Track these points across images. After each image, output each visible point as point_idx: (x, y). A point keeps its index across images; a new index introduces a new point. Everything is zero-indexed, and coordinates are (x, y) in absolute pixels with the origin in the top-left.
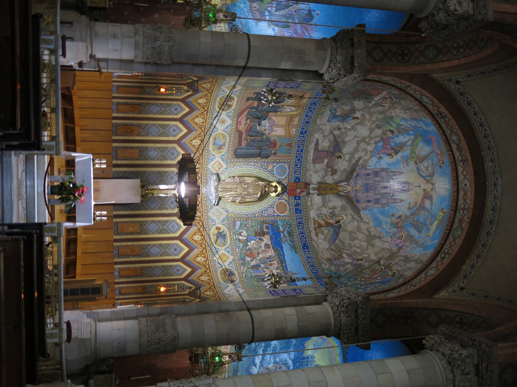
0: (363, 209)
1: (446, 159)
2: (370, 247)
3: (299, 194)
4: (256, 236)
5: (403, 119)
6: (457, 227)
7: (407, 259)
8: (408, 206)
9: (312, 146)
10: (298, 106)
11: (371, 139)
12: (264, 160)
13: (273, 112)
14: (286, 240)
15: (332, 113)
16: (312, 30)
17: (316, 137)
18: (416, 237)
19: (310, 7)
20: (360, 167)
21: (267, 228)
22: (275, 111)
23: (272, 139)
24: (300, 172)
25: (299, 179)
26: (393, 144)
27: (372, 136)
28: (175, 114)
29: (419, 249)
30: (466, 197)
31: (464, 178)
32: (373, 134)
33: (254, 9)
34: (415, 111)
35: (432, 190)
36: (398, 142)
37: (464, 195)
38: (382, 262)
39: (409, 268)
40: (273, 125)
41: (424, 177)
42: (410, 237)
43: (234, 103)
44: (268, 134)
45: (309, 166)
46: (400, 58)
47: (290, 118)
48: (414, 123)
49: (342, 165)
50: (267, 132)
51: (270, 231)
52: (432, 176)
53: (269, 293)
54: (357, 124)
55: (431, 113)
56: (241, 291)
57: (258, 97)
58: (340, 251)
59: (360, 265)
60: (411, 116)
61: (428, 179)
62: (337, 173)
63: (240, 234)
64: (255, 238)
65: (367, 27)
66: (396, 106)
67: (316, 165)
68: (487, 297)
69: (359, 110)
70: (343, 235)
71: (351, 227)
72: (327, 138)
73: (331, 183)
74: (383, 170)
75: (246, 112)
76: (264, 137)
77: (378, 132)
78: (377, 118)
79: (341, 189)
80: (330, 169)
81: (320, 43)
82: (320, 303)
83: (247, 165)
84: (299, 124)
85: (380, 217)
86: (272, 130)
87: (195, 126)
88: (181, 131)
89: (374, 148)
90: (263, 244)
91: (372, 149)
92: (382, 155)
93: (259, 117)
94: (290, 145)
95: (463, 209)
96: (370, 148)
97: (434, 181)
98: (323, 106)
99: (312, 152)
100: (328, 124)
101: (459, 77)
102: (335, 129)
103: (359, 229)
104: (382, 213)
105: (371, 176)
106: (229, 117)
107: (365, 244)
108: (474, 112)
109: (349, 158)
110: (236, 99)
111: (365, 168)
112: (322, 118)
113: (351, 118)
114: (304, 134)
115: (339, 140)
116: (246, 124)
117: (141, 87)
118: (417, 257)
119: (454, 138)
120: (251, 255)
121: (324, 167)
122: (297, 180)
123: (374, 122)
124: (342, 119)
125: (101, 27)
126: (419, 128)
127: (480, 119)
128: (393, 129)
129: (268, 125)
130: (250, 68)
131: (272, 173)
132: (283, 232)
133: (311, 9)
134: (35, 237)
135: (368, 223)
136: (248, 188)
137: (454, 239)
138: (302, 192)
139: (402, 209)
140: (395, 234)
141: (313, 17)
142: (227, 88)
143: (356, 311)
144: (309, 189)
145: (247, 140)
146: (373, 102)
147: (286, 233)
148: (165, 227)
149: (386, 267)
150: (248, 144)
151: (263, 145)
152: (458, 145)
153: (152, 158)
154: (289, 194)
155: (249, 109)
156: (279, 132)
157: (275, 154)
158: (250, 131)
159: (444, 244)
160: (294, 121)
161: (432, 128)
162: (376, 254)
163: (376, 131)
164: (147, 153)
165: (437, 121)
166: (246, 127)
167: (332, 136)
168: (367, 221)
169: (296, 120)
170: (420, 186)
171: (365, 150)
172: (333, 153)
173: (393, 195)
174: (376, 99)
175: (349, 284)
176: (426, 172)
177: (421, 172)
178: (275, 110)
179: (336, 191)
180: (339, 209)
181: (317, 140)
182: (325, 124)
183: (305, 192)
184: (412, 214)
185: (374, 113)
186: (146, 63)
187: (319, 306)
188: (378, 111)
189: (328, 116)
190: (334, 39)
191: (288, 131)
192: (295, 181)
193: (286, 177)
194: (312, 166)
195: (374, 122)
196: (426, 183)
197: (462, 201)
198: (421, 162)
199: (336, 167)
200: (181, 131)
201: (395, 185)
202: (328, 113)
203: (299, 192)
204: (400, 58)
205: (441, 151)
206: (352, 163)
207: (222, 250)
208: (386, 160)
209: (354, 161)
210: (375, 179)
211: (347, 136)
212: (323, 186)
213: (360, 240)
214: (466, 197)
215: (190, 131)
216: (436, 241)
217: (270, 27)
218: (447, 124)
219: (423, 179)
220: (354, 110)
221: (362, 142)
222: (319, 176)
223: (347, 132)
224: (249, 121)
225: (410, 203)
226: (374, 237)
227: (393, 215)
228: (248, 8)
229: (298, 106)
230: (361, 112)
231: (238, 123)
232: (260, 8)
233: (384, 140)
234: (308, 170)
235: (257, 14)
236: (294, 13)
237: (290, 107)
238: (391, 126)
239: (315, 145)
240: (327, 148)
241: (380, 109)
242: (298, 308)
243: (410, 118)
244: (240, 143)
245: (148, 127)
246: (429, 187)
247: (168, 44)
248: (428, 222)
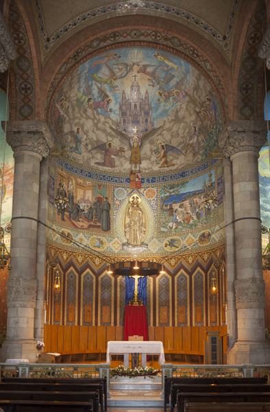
0: (153, 126)
1: (113, 52)
2: (185, 120)
3: (139, 179)
4: (172, 215)
6: (171, 42)
7: (196, 88)
9: (100, 168)
11: (95, 118)
14: (177, 190)
18: (178, 80)
21: (166, 206)
22: (73, 198)
26: (100, 99)
27: (92, 117)
28: (76, 278)
29: (188, 78)
30: (146, 34)
31: (130, 36)
34: (72, 79)
35: (138, 66)
36: (98, 95)
37: (144, 35)
38: (198, 110)
39: (204, 86)
40: (83, 200)
41: (127, 73)
42: (178, 85)
43: (67, 231)
46: (29, 92)
48: (82, 81)
49: (116, 143)
51: (169, 204)
52: (126, 65)
53: (221, 204)
54: (83, 130)
55: (74, 65)
56: (217, 227)
57: (62, 211)
58: (187, 146)
59: (199, 129)
61: (129, 68)
63: (171, 228)
64: (174, 217)
65: (3, 120)
66: (68, 96)
68: (233, 14)
69: (72, 128)
70: (174, 143)
71: (167, 136)
73: (130, 152)
74: (121, 108)
77: (89, 112)
79: (135, 145)
81: (17, 159)
82: (232, 163)
85: (159, 111)
86: (88, 200)
87: (84, 263)
88: (88, 273)
90: (180, 209)
91: (103, 117)
94: (100, 186)
95: (156, 36)
96: (102, 119)
99: (105, 168)
102: (87, 149)
103: (169, 130)
104: (157, 111)
106: (77, 235)
107: (182, 124)
108: (73, 25)
110: (63, 229)
116: (83, 222)
117: (54, 304)
118: (195, 79)
119: (95, 44)
120: (188, 220)
123: (81, 116)
125: (11, 333)
127: (79, 19)
128: (86, 100)
129: (84, 204)
130: (38, 217)
132: (170, 193)
134: (175, 385)
135: (165, 122)
136: (134, 221)
137: (181, 45)
138: (138, 177)
139: (154, 92)
140: (174, 98)
142: (54, 236)
143: (239, 132)
146: (65, 115)
147: (171, 191)
148: (164, 287)
149: (202, 106)
150: (99, 221)
152: (101, 41)
154: (140, 188)
156: (89, 195)
157: (107, 198)
158: (88, 219)
159: (185, 55)
161: (87, 65)
162: (191, 115)
165: (81, 60)
168: (163, 123)
170: (135, 76)
172: (107, 151)
173: (142, 99)
174: (62, 113)
175: (215, 138)
176: (123, 70)
178: (72, 198)
180: (152, 146)
181: (96, 163)
183: (139, 174)
184: (158, 83)
186: (37, 299)
187: (234, 164)
190: (14, 148)
194: (117, 168)
197: (149, 37)
199: (118, 148)
200: (88, 273)
201: (133, 96)
204: (29, 92)
205: (107, 56)
207: (184, 242)
208: (113, 105)
209: (113, 133)
211: (92, 138)
212: (133, 158)
213: (179, 128)
214: (146, 34)
215: (88, 266)
216: (182, 62)
218: (83, 50)
219: (130, 73)
220: (72, 132)
224: (80, 219)
226: (176, 116)
227: (159, 100)
229: (69, 179)
230: (73, 126)
231: (82, 228)
233: (96, 106)
241: (70, 110)
242: (235, 181)
244: (99, 227)
246: (135, 67)
248: (165, 69)
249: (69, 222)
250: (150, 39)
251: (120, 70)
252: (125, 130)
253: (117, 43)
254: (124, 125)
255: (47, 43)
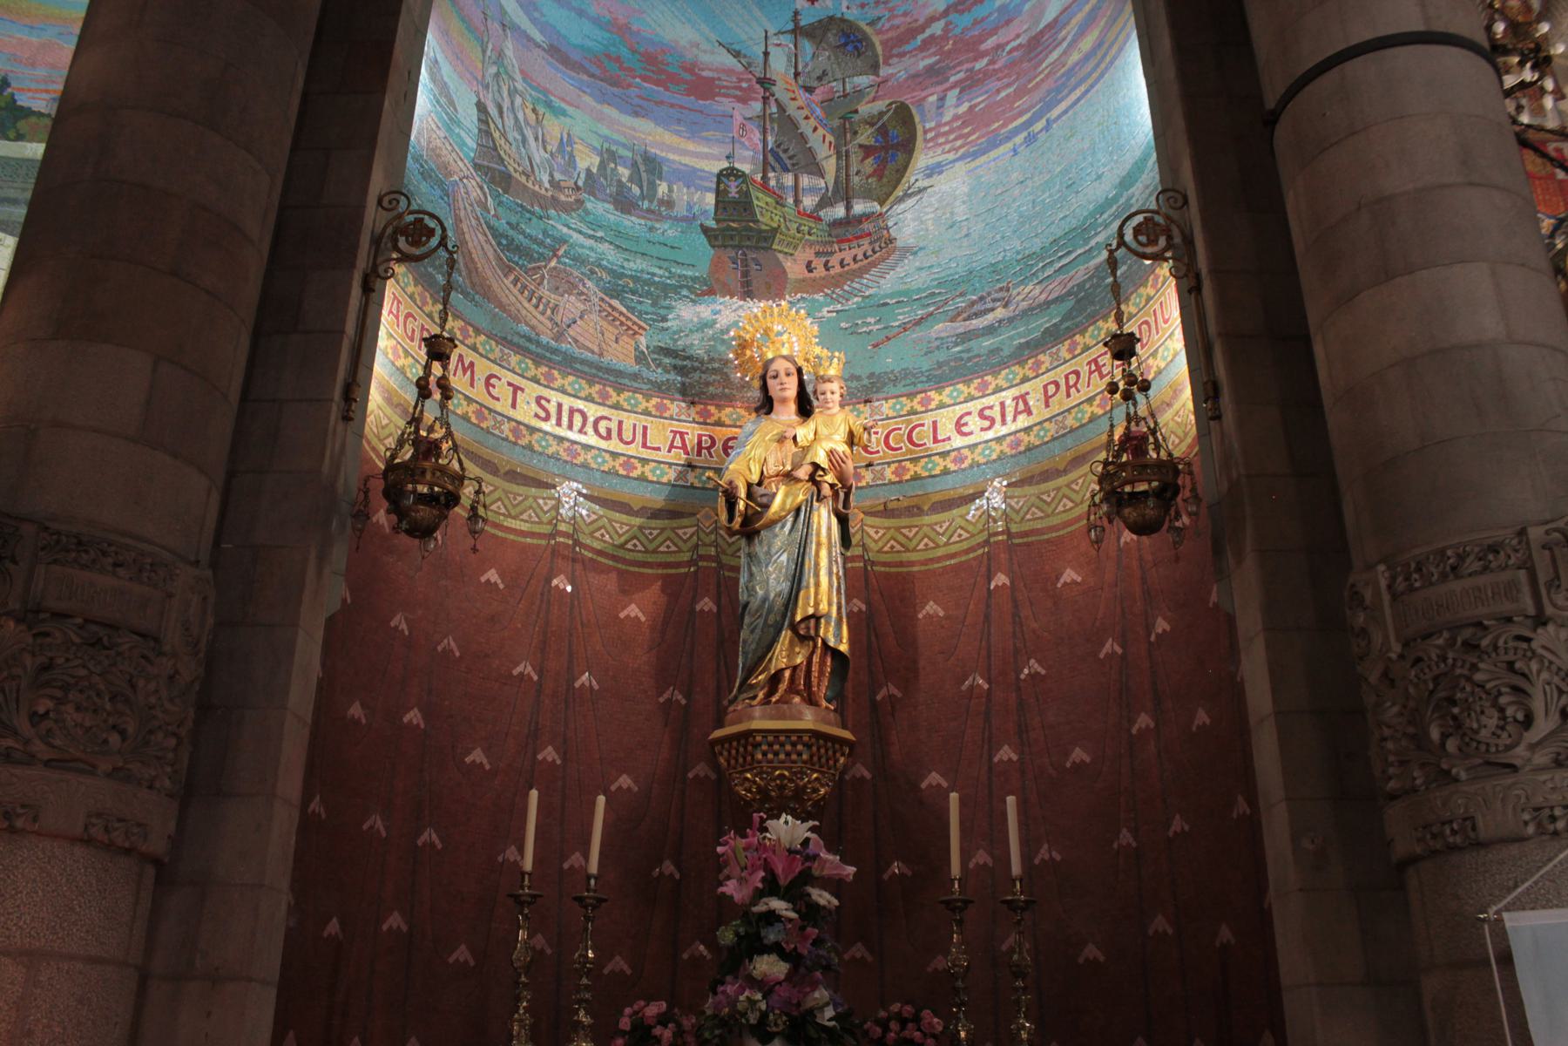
16: (905, 14)
19: (780, 33)
33: (820, 272)
133: (791, 26)
141: (831, 18)
217: (921, 191)
228: (819, 297)
232: (811, 244)
235: (847, 256)
236: (818, 96)
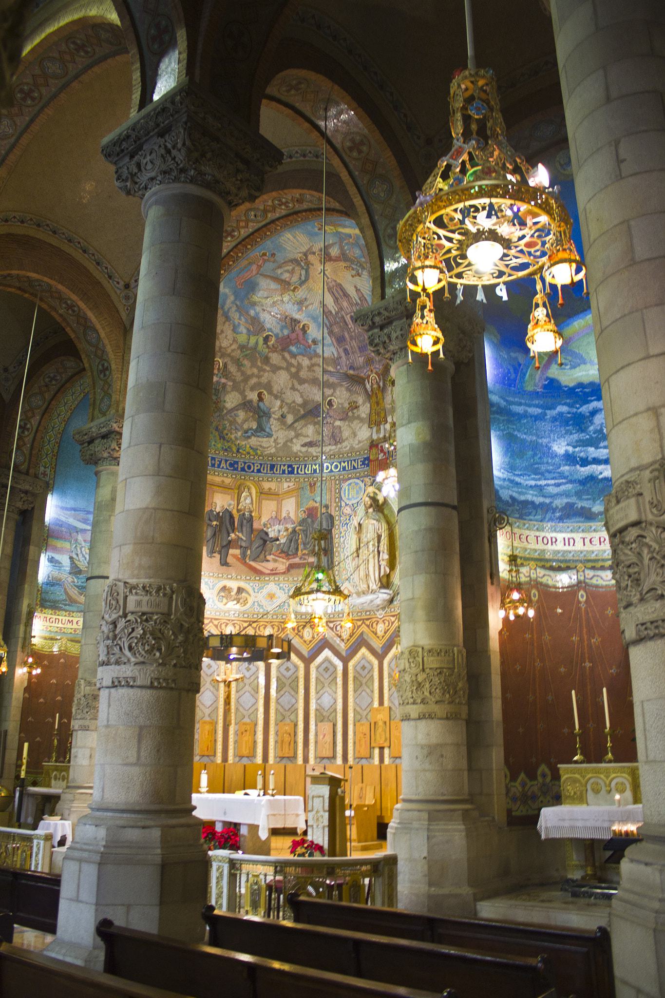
1: (255, 253)
5: (235, 329)
8: (358, 277)
10: (239, 488)
11: (290, 365)
12: (336, 523)
13: (252, 524)
15: (253, 434)
17: (299, 449)
20: (339, 367)
22: (251, 520)
23: (304, 516)
24: (355, 460)
25: (365, 459)
27: (284, 365)
32: (282, 365)
35: (314, 253)
44: (293, 523)
45: (345, 448)
46: (107, 373)
47: (263, 495)
48: (234, 315)
50: (290, 526)
52: (295, 261)
54: (270, 392)
60: (224, 323)
62: (355, 400)
67: (344, 438)
72: (300, 432)
73: (369, 406)
74: (331, 333)
75: (252, 563)
76: (300, 530)
77: (275, 358)
78: (251, 367)
80: (350, 414)
83: (344, 549)
84: (275, 480)
86: (287, 519)
89: (304, 356)
91: (305, 358)
92: (310, 341)
93: (261, 542)
96: (306, 362)
97: (300, 255)
98: (238, 451)
100: (275, 437)
101: (118, 288)
105: (347, 347)
106: (262, 588)
109: (330, 389)
111: (337, 359)
112: (264, 448)
113: (261, 404)
114: (293, 469)
115: (302, 412)
116: (275, 561)
121: (347, 423)
122: (366, 462)
124: (264, 418)
126: (237, 305)
129: (277, 527)
131: (355, 505)
138: (382, 451)
144: (379, 439)
145: (304, 554)
146: (223, 380)
151: (312, 527)
153: (332, 701)
155: (247, 559)
158: (285, 553)
160: (270, 489)
163: (274, 362)
164: (326, 709)
166: (281, 559)
167: (296, 425)
169: (266, 485)
171: (310, 368)
173: (357, 304)
177: (303, 278)
179: (380, 395)
181: (303, 446)
182: (275, 441)
185: (243, 373)
188: (239, 370)
189: (260, 439)
191: (289, 494)
192: (368, 465)
193: (362, 481)
194: (344, 444)
195: (261, 370)
196: (312, 265)
198: (289, 283)
199: (346, 405)
202: (254, 441)
203: (382, 454)
204: (107, 373)
205: (250, 264)
206: (336, 381)
208: (314, 332)
210: (348, 339)
211: (294, 402)
212: (374, 417)
220: (246, 405)
221: (299, 376)
222: (360, 428)
223: (287, 404)
224: (268, 557)
225: (353, 276)
231: (274, 573)
234: (352, 448)
237: (242, 499)
238: (257, 343)
239: (312, 447)
240: (317, 426)
241: (232, 368)
243: (227, 323)
245: (282, 710)
247: (82, 687)
249: (243, 567)
250: (284, 213)
251: (292, 272)
252: (352, 368)
253: (243, 240)
254: (348, 359)
255: (127, 291)
